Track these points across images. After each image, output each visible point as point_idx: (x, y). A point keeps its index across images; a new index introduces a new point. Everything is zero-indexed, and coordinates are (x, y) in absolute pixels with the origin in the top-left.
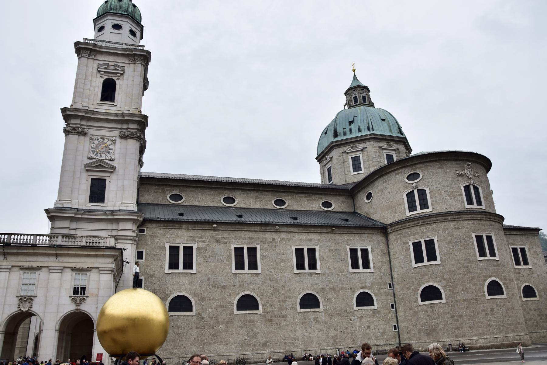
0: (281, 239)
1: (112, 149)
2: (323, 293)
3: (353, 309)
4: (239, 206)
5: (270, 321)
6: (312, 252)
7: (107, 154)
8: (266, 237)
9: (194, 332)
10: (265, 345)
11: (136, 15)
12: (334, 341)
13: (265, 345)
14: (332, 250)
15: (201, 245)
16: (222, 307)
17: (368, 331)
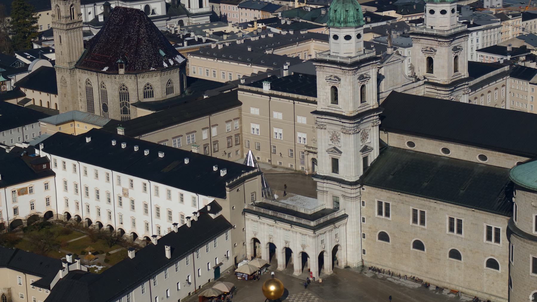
0: (441, 209)
1: (340, 139)
2: (464, 251)
3: (483, 267)
4: (452, 157)
5: (431, 260)
6: (460, 222)
7: (337, 142)
8: (431, 205)
9: (391, 254)
10: (427, 273)
11: (348, 19)
12: (469, 284)
13: (427, 273)
14: (474, 224)
15: (394, 204)
16: (405, 244)
17: (492, 285)
